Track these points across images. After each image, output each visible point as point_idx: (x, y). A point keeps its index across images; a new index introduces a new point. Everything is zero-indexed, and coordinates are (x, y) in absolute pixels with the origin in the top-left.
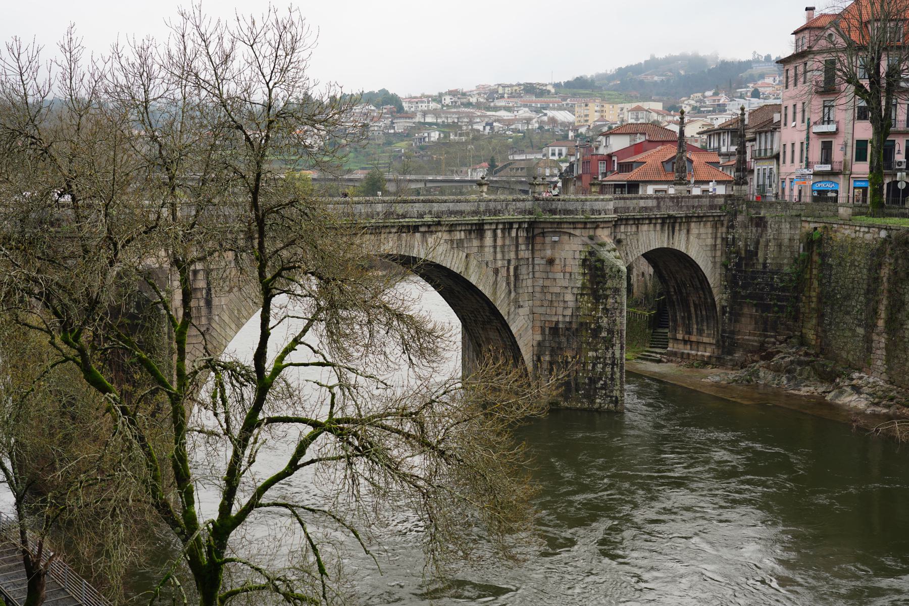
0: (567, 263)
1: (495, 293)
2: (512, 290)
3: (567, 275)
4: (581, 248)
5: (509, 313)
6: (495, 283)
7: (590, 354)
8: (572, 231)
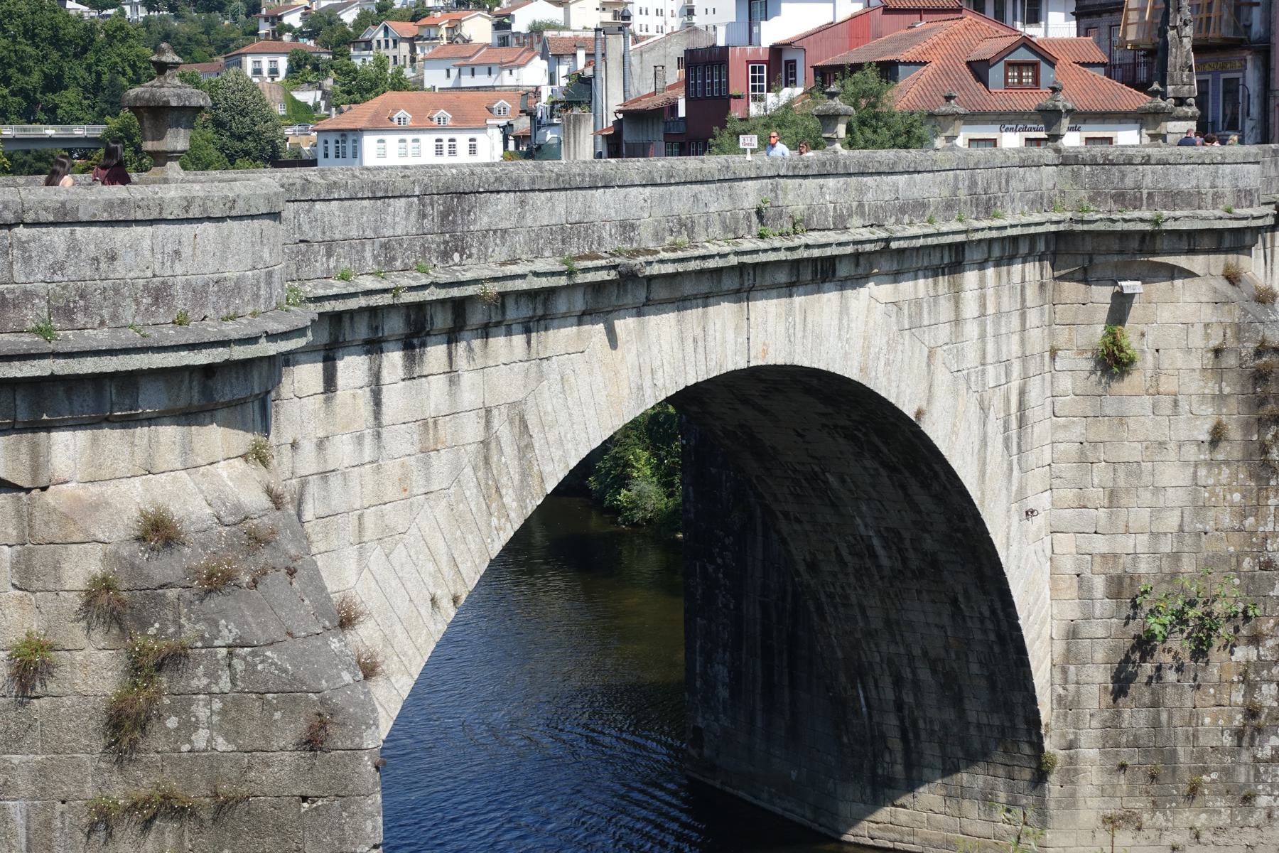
0: (1166, 364)
3: (1166, 402)
4: (1207, 314)
7: (1243, 653)
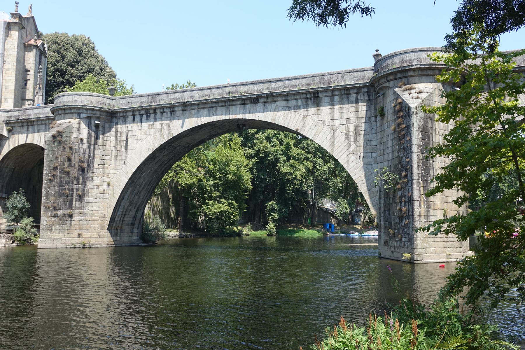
1: (333, 144)
2: (352, 143)
5: (348, 161)
6: (333, 137)
8: (387, 84)
